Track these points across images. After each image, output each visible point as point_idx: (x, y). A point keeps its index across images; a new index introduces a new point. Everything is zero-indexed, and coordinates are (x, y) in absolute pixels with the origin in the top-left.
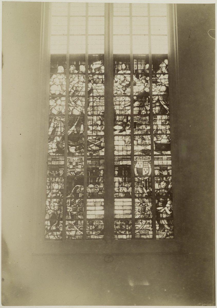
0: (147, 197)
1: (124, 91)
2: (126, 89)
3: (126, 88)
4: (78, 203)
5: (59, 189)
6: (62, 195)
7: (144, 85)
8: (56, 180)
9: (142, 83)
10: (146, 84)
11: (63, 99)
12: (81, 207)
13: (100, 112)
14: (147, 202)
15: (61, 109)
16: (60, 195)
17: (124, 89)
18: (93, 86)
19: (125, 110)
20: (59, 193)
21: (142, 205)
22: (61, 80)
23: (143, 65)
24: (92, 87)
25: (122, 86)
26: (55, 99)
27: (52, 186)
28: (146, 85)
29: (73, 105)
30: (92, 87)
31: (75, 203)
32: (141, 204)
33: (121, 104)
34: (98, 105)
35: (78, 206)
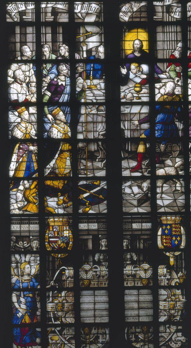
0: (176, 287)
1: (138, 92)
2: (141, 90)
3: (141, 87)
4: (65, 296)
5: (32, 274)
6: (38, 284)
7: (174, 82)
8: (27, 259)
9: (171, 78)
10: (177, 79)
11: (33, 110)
12: (71, 302)
13: (99, 134)
14: (178, 295)
15: (29, 130)
16: (34, 284)
17: (138, 89)
18: (85, 84)
19: (141, 129)
20: (32, 281)
21: (170, 300)
22: (27, 73)
23: (172, 43)
24: (83, 86)
25: (134, 84)
26: (18, 110)
27: (19, 269)
28: (176, 82)
29: (51, 121)
30: (83, 86)
31: (61, 297)
32: (168, 297)
33: (133, 119)
34: (95, 120)
35: (65, 301)
